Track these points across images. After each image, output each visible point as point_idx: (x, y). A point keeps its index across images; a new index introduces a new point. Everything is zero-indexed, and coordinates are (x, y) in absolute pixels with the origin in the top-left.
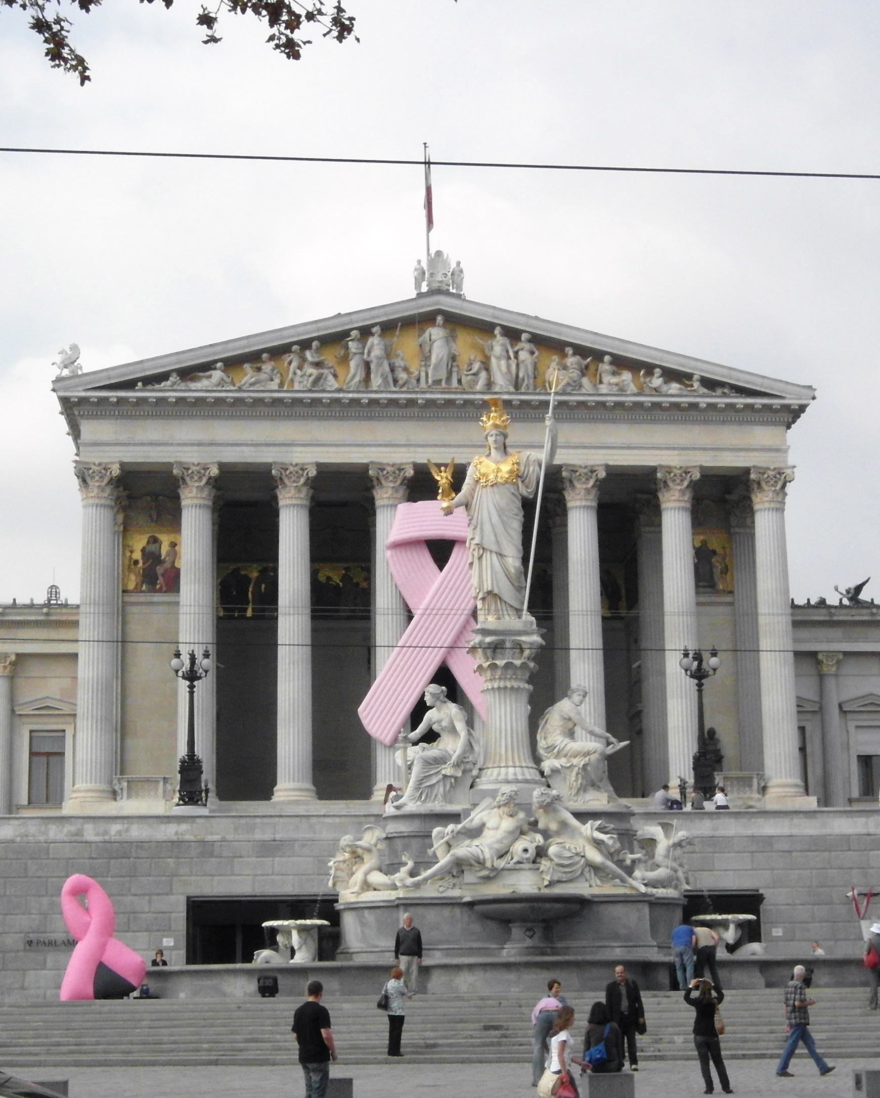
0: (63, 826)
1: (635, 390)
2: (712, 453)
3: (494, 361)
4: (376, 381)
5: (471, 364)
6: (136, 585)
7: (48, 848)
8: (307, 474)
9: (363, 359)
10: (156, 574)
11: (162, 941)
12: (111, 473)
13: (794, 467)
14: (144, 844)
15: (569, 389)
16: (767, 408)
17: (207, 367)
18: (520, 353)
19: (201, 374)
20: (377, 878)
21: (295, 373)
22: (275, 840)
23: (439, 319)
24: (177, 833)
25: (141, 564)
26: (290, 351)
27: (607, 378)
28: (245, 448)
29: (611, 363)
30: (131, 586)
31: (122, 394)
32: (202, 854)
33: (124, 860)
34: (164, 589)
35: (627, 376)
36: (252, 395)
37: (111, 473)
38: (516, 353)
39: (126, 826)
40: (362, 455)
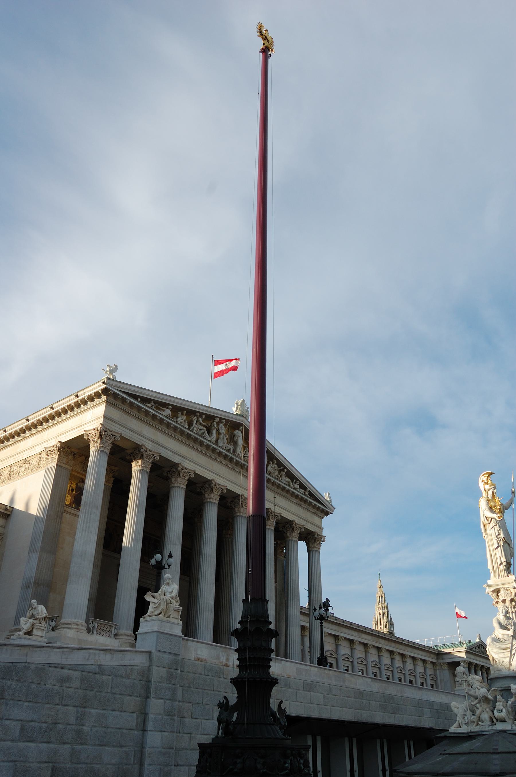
1: (293, 487)
2: (306, 522)
4: (221, 444)
6: (70, 503)
12: (115, 438)
13: (325, 536)
15: (276, 477)
16: (322, 511)
17: (165, 405)
25: (74, 492)
28: (169, 452)
29: (285, 473)
30: (67, 503)
31: (133, 400)
35: (288, 480)
36: (181, 428)
37: (115, 438)
40: (208, 475)
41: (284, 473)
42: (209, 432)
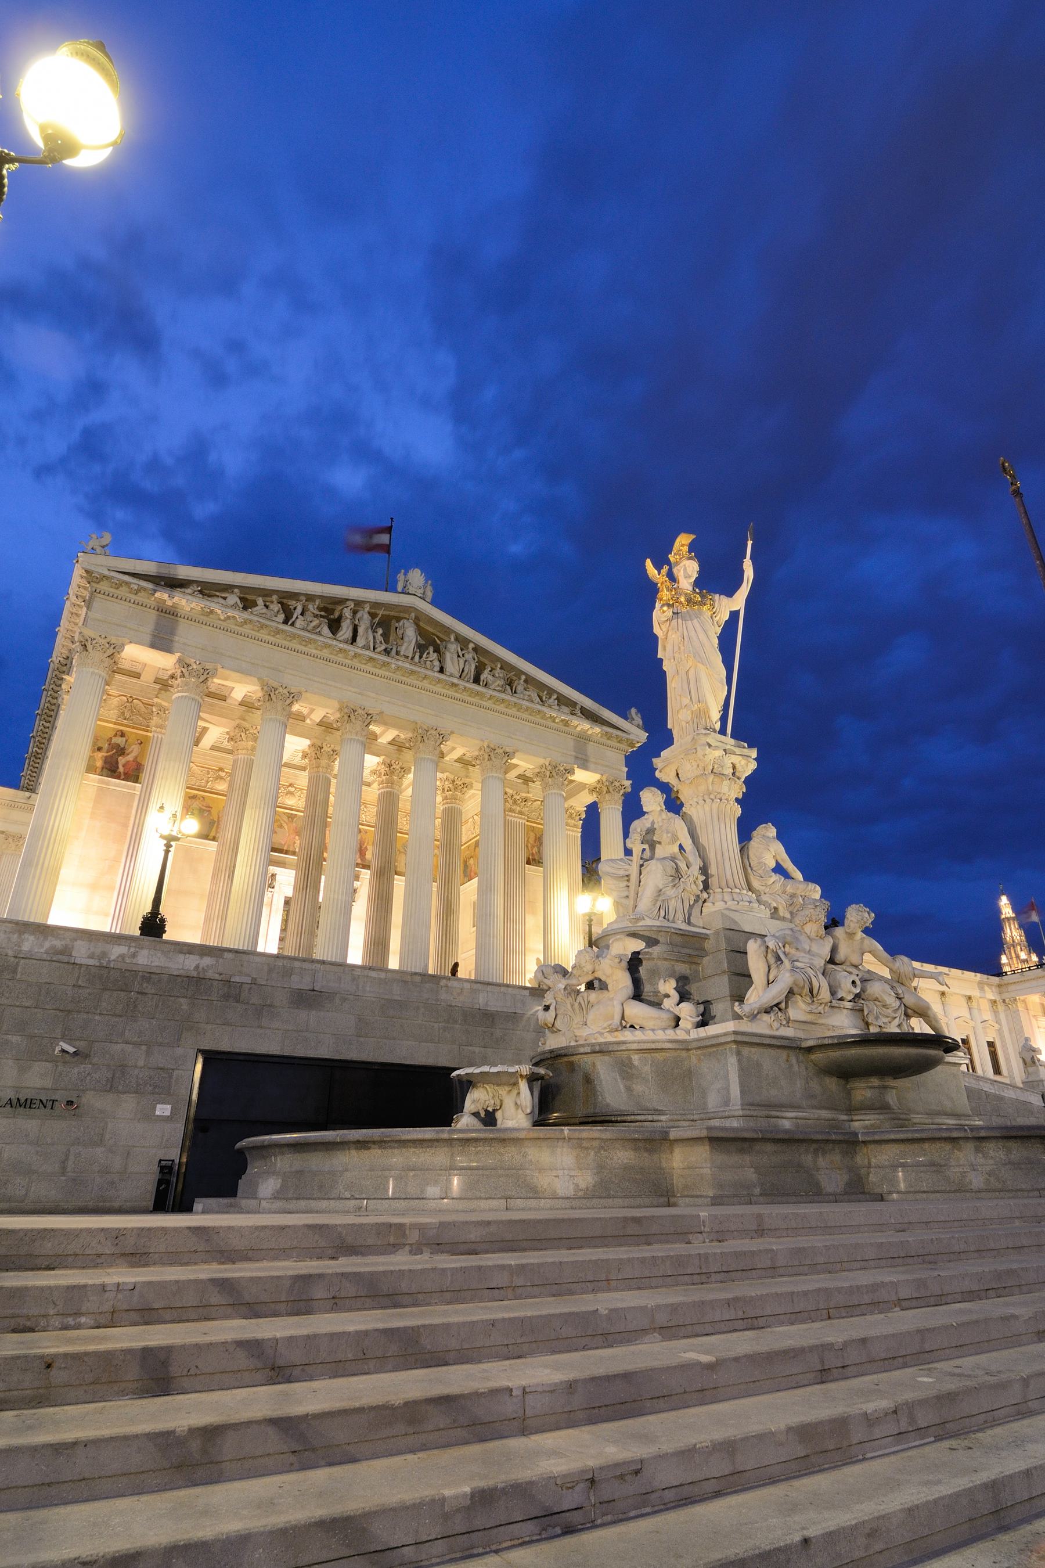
0: (46, 938)
3: (448, 656)
4: (360, 641)
5: (428, 654)
7: (17, 964)
8: (293, 697)
9: (355, 624)
10: (117, 763)
11: (155, 1108)
14: (153, 976)
18: (466, 656)
19: (218, 594)
20: (637, 1011)
21: (297, 618)
22: (314, 990)
23: (413, 615)
24: (197, 967)
26: (298, 600)
27: (520, 688)
32: (226, 997)
33: (122, 994)
34: (123, 777)
36: (261, 620)
38: (463, 655)
39: (132, 950)
41: (522, 681)
42: (335, 626)
